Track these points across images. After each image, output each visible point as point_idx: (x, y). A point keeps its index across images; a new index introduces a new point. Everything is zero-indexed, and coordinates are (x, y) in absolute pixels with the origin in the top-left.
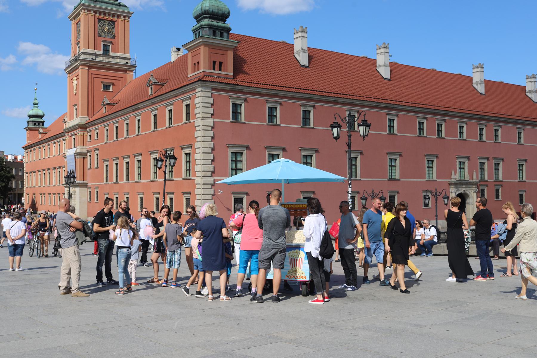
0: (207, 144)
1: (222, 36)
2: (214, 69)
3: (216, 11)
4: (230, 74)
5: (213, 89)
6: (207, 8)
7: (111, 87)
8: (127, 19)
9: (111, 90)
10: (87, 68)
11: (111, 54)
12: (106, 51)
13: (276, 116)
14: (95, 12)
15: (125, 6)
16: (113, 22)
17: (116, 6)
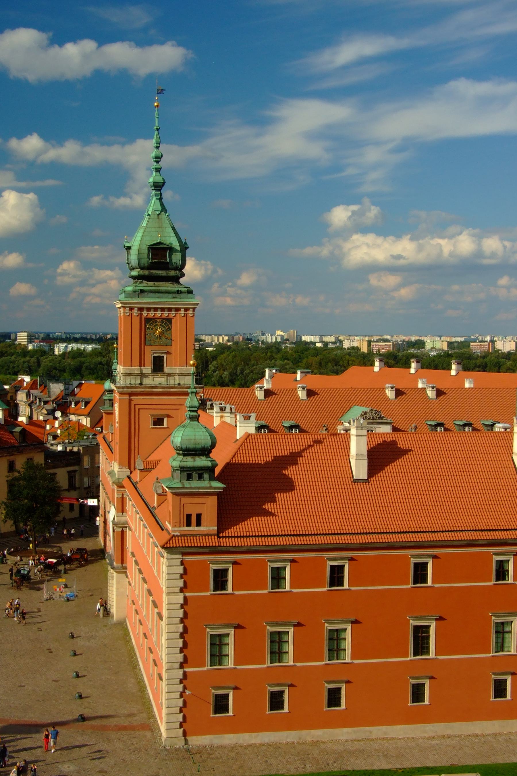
0: (173, 628)
1: (200, 477)
2: (189, 524)
3: (191, 446)
4: (211, 528)
5: (183, 554)
6: (179, 445)
7: (165, 419)
8: (190, 312)
9: (165, 425)
10: (127, 397)
11: (166, 370)
12: (158, 366)
13: (285, 578)
14: (141, 309)
15: (190, 292)
16: (169, 320)
17: (174, 295)
